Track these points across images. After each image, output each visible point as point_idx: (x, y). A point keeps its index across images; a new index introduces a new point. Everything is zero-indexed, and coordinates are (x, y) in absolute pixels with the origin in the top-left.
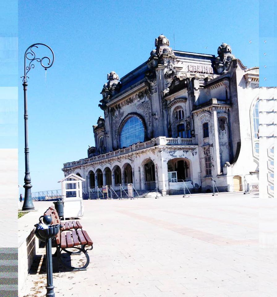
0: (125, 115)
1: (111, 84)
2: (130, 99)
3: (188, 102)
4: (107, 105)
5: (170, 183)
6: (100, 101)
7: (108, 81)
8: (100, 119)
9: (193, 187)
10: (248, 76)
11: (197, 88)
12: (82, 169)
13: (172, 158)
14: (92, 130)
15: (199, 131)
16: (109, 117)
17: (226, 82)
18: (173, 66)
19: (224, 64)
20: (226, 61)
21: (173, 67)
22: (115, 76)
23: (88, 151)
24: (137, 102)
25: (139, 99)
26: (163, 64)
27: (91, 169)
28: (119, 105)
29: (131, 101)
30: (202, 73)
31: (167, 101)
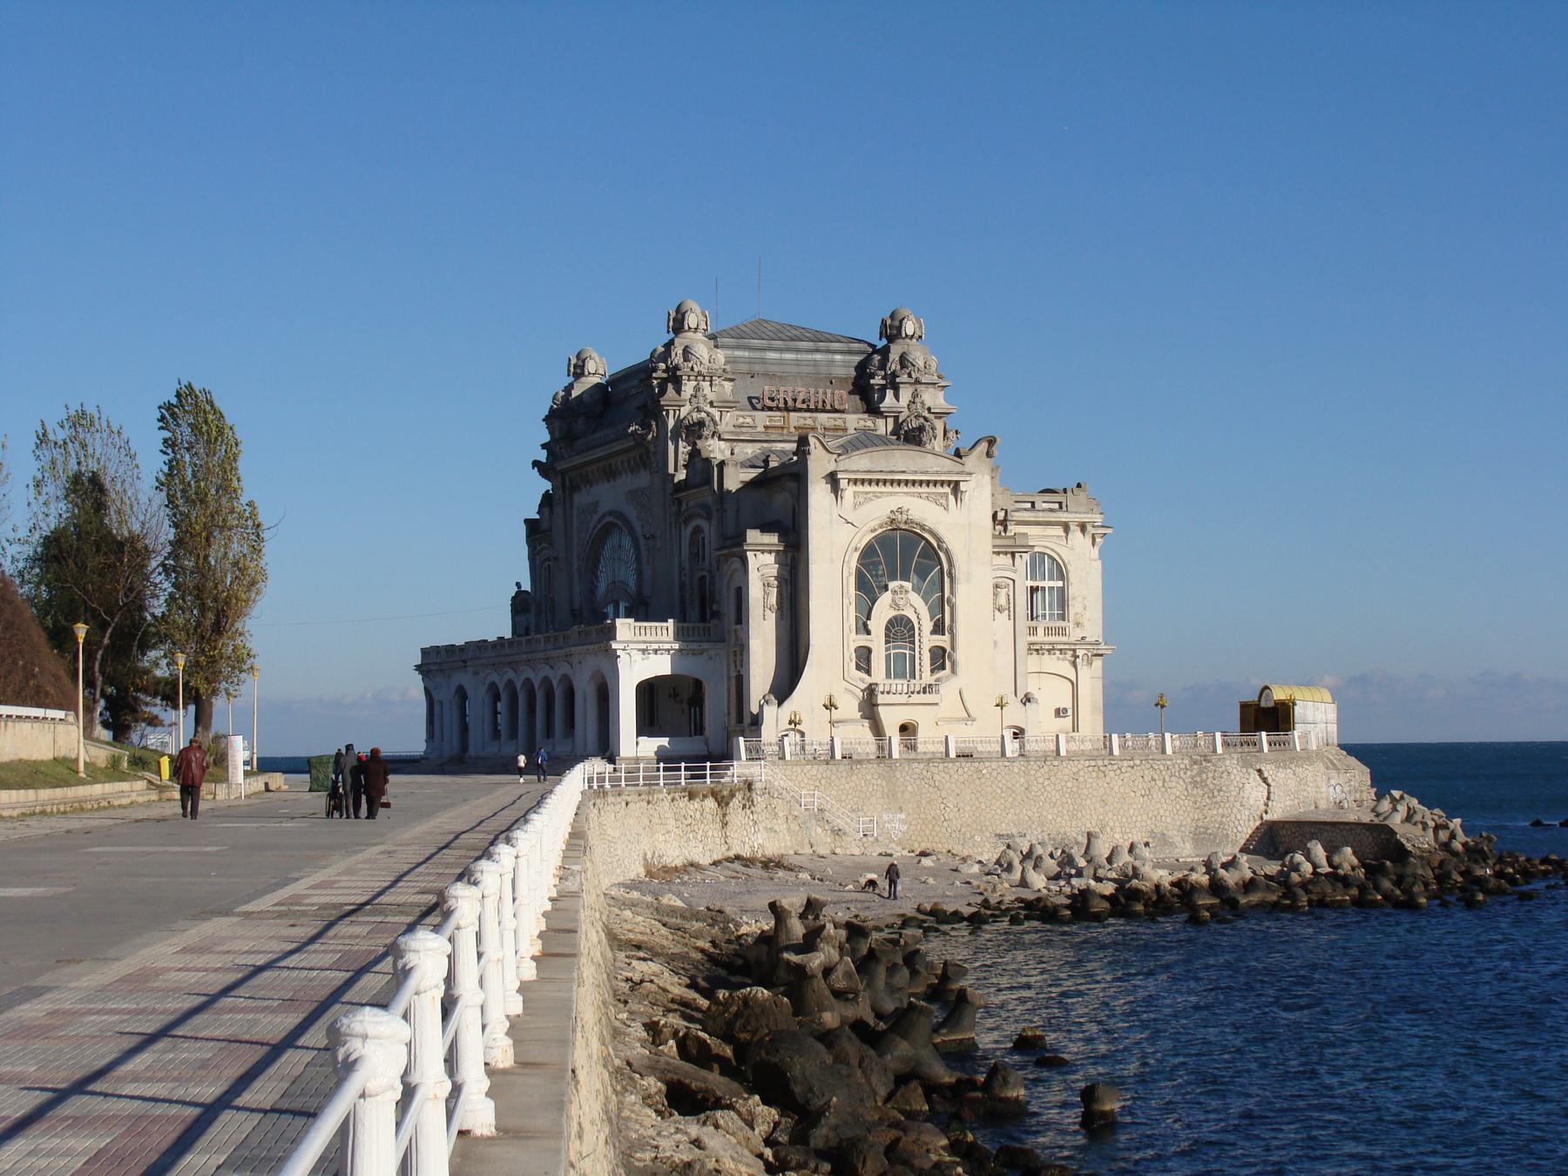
0: (601, 511)
1: (575, 393)
3: (714, 522)
4: (560, 466)
5: (642, 739)
6: (544, 446)
8: (547, 499)
17: (791, 485)
18: (711, 397)
22: (590, 366)
24: (628, 482)
26: (678, 391)
27: (494, 677)
29: (611, 474)
30: (808, 410)
31: (680, 502)
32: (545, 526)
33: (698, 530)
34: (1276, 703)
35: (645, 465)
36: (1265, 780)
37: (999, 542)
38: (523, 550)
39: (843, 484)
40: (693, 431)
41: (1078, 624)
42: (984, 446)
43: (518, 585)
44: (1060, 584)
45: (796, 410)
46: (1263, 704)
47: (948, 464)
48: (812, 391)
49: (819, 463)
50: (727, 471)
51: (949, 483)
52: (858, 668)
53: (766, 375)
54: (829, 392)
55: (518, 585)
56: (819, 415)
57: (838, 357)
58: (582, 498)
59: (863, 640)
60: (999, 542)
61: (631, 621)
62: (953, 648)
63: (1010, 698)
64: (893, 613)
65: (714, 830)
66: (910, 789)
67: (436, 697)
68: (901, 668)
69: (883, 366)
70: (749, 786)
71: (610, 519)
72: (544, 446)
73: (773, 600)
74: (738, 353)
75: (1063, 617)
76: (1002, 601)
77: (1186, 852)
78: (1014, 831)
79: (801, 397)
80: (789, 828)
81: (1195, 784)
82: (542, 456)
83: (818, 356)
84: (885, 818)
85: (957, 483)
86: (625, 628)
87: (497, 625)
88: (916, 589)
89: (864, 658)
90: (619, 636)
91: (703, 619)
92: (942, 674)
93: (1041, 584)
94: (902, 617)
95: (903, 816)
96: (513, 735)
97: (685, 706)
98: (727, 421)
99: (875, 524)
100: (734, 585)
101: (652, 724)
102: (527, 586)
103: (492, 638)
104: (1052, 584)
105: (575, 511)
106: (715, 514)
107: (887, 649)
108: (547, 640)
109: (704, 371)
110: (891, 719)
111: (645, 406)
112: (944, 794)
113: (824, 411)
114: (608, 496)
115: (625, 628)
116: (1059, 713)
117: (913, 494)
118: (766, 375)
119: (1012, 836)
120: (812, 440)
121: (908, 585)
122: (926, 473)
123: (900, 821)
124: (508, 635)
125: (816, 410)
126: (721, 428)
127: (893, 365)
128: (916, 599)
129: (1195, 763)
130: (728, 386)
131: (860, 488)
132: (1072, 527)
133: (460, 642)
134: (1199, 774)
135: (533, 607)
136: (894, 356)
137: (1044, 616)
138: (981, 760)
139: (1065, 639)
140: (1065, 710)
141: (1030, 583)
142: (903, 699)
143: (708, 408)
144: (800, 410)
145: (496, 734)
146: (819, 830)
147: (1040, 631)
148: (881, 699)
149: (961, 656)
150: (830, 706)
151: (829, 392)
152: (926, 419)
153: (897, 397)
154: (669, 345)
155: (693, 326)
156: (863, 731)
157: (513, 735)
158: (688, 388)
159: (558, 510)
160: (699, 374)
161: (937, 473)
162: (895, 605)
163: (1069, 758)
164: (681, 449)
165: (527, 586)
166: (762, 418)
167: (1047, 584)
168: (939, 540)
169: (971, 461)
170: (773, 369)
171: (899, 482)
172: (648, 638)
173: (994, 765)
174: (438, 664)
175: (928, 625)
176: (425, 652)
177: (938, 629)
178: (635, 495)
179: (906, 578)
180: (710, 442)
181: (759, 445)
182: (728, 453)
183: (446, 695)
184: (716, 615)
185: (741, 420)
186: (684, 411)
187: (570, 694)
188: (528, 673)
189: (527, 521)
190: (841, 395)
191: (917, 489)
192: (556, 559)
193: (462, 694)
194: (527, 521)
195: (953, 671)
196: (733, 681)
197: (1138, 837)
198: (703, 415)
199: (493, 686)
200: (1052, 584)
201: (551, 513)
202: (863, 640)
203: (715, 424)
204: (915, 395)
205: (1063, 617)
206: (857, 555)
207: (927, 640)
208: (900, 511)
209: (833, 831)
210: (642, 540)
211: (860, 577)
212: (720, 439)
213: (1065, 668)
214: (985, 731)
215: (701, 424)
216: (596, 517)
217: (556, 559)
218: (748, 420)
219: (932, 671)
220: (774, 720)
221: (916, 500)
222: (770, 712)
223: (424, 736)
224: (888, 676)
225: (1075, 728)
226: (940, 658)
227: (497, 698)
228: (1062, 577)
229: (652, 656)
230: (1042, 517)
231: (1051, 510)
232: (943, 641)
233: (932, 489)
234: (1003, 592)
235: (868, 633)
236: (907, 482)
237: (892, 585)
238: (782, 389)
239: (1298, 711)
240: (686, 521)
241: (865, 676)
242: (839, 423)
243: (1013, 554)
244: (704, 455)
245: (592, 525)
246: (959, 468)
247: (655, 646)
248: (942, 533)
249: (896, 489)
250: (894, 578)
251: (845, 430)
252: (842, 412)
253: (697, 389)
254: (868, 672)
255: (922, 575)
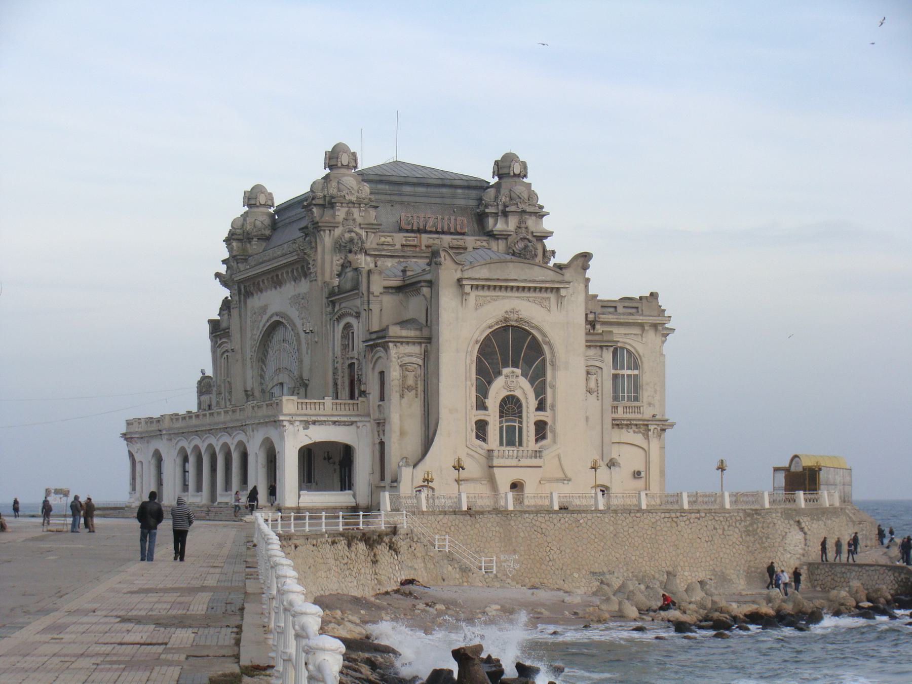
0: (269, 314)
2: (277, 276)
5: (302, 492)
6: (224, 262)
7: (246, 209)
8: (226, 305)
9: (354, 504)
10: (464, 282)
11: (376, 293)
12: (165, 441)
13: (307, 442)
14: (207, 328)
15: (372, 387)
16: (240, 307)
17: (425, 290)
18: (359, 220)
19: (498, 209)
20: (504, 199)
21: (357, 224)
23: (200, 383)
24: (290, 289)
25: (293, 283)
26: (334, 216)
28: (258, 283)
29: (277, 283)
30: (437, 232)
31: (333, 303)
32: (224, 325)
33: (348, 326)
34: (804, 469)
35: (306, 275)
36: (802, 529)
37: (590, 338)
38: (207, 343)
39: (467, 289)
40: (346, 247)
41: (650, 404)
42: (580, 261)
43: (203, 372)
44: (636, 372)
45: (426, 232)
46: (793, 469)
47: (551, 275)
48: (440, 217)
49: (448, 273)
50: (375, 278)
51: (552, 289)
52: (478, 437)
53: (402, 203)
54: (453, 218)
55: (203, 372)
56: (441, 236)
57: (459, 191)
58: (255, 302)
59: (481, 415)
60: (590, 338)
61: (295, 398)
62: (554, 424)
63: (600, 462)
64: (505, 393)
65: (367, 569)
66: (522, 534)
67: (138, 458)
68: (512, 438)
69: (496, 197)
70: (394, 531)
71: (277, 318)
72: (224, 262)
73: (410, 381)
74: (380, 186)
75: (636, 399)
76: (592, 384)
77: (741, 587)
78: (605, 569)
79: (431, 223)
80: (426, 567)
81: (748, 533)
82: (223, 269)
83: (444, 190)
84: (502, 558)
85: (558, 289)
86: (289, 404)
87: (187, 401)
88: (525, 375)
89: (481, 428)
90: (285, 411)
91: (352, 397)
92: (544, 442)
93: (621, 372)
94: (513, 397)
95: (516, 557)
96: (199, 488)
97: (337, 467)
98: (371, 242)
99: (491, 321)
100: (377, 370)
101: (309, 481)
102: (209, 372)
103: (182, 412)
104: (630, 372)
105: (249, 314)
106: (363, 314)
107: (501, 422)
108: (226, 412)
109: (354, 199)
110: (504, 478)
111: (306, 227)
112: (549, 539)
113: (451, 234)
114: (275, 301)
115: (289, 404)
116: (637, 475)
117: (522, 298)
118: (402, 203)
119: (603, 574)
120: (442, 254)
121: (518, 371)
122: (534, 281)
123: (516, 561)
124: (195, 409)
125: (443, 233)
126: (368, 245)
127: (504, 199)
128: (524, 383)
129: (749, 515)
130: (373, 213)
131: (481, 293)
132: (646, 328)
133: (156, 415)
134: (751, 524)
135: (215, 389)
136: (504, 191)
137: (623, 397)
138: (573, 512)
139: (639, 416)
140: (639, 473)
141: (614, 372)
142: (514, 462)
143: (357, 230)
144: (431, 232)
145: (185, 487)
146: (450, 568)
147: (620, 410)
148: (496, 462)
149: (560, 428)
150: (459, 467)
151: (453, 218)
152: (530, 241)
153: (507, 223)
154: (326, 178)
155: (345, 163)
156: (482, 489)
157: (199, 488)
158: (341, 213)
159: (235, 313)
160: (351, 202)
161: (542, 281)
162: (507, 387)
163: (648, 511)
164: (335, 263)
165: (209, 372)
166: (399, 239)
167: (626, 372)
168: (544, 335)
169: (568, 275)
170: (406, 199)
171: (512, 288)
172: (309, 412)
173: (589, 516)
174: (141, 433)
175: (533, 403)
176: (129, 423)
177: (541, 407)
178: (297, 300)
179: (515, 365)
180: (359, 256)
181: (397, 260)
182: (372, 266)
183: (145, 456)
184: (363, 393)
185: (383, 239)
186: (337, 232)
187: (244, 457)
188: (212, 440)
189: (210, 321)
190: (464, 222)
191: (526, 294)
192: (233, 350)
193: (158, 459)
194: (210, 321)
195: (554, 441)
196: (377, 446)
197: (701, 575)
198: (353, 235)
199: (183, 451)
200: (630, 372)
201: (230, 315)
202: (481, 415)
203: (363, 242)
204: (520, 223)
205: (636, 399)
206: (477, 346)
207: (530, 416)
208: (513, 311)
209: (461, 569)
210: (302, 335)
211: (479, 361)
212: (366, 254)
213: (638, 439)
214: (580, 489)
215: (351, 240)
216: (265, 318)
217: (233, 350)
218: (389, 239)
219: (537, 441)
220: (409, 479)
221: (525, 303)
222: (406, 473)
223: (128, 487)
224: (501, 444)
225: (647, 487)
226: (541, 428)
227: (186, 460)
228: (636, 368)
229: (311, 427)
230: (623, 319)
231: (631, 314)
232: (541, 416)
233: (538, 295)
234: (593, 377)
235: (485, 408)
236: (518, 288)
237: (505, 371)
238: (415, 215)
239: (823, 475)
240: (339, 319)
241: (482, 443)
242: (461, 243)
243: (601, 347)
244: (354, 266)
245: (261, 325)
246: (559, 278)
247: (314, 418)
248: (547, 329)
249: (509, 294)
250: (506, 365)
251: (466, 249)
252: (463, 234)
253: (348, 213)
254: (484, 440)
255: (529, 362)
